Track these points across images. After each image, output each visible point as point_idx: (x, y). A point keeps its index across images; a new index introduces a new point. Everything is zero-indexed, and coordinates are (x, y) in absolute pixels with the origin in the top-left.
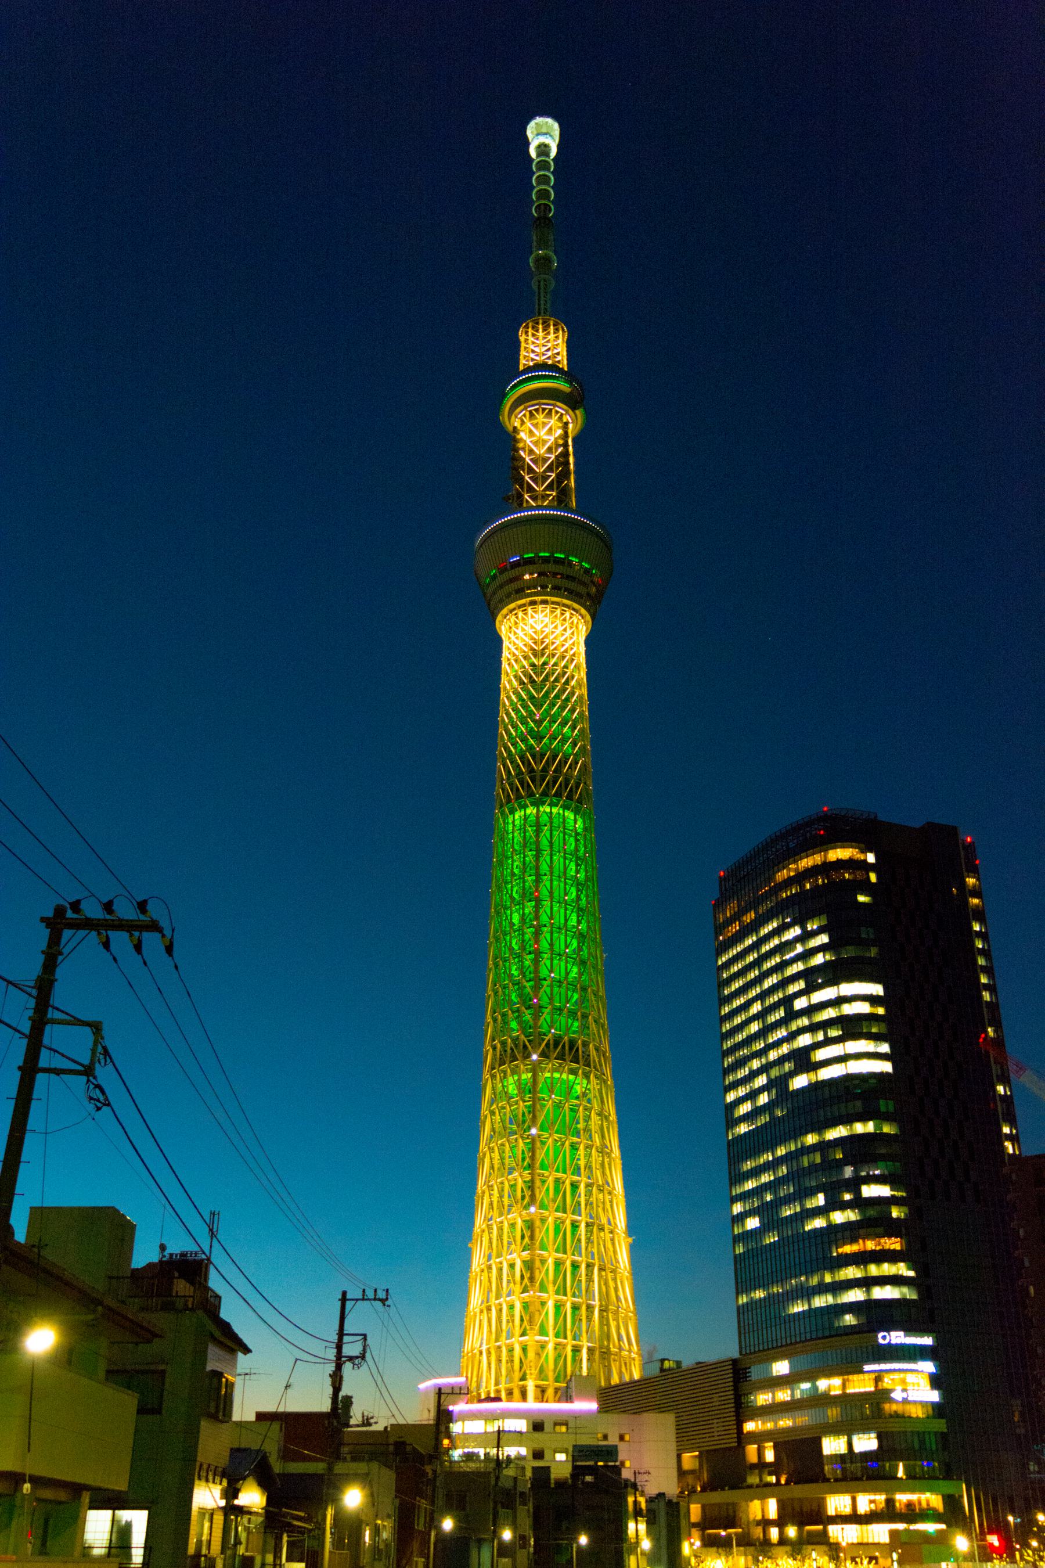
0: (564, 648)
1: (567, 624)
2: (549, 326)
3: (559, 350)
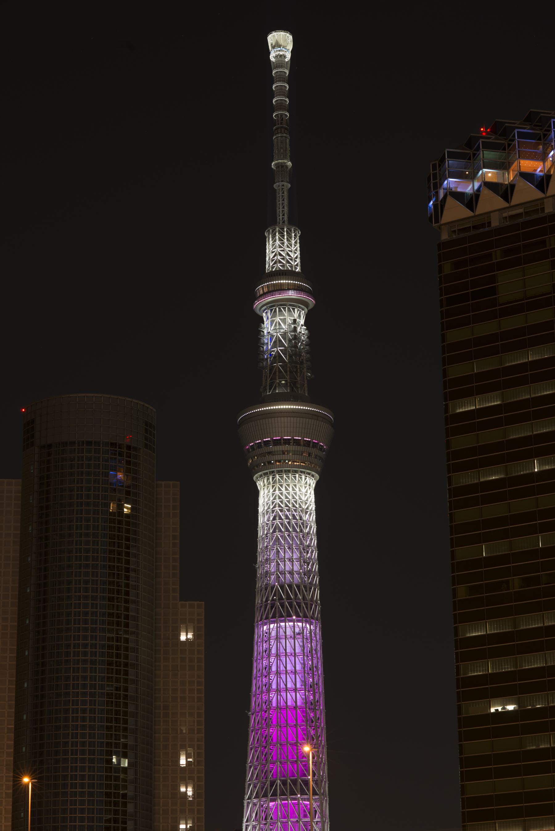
2: (275, 234)
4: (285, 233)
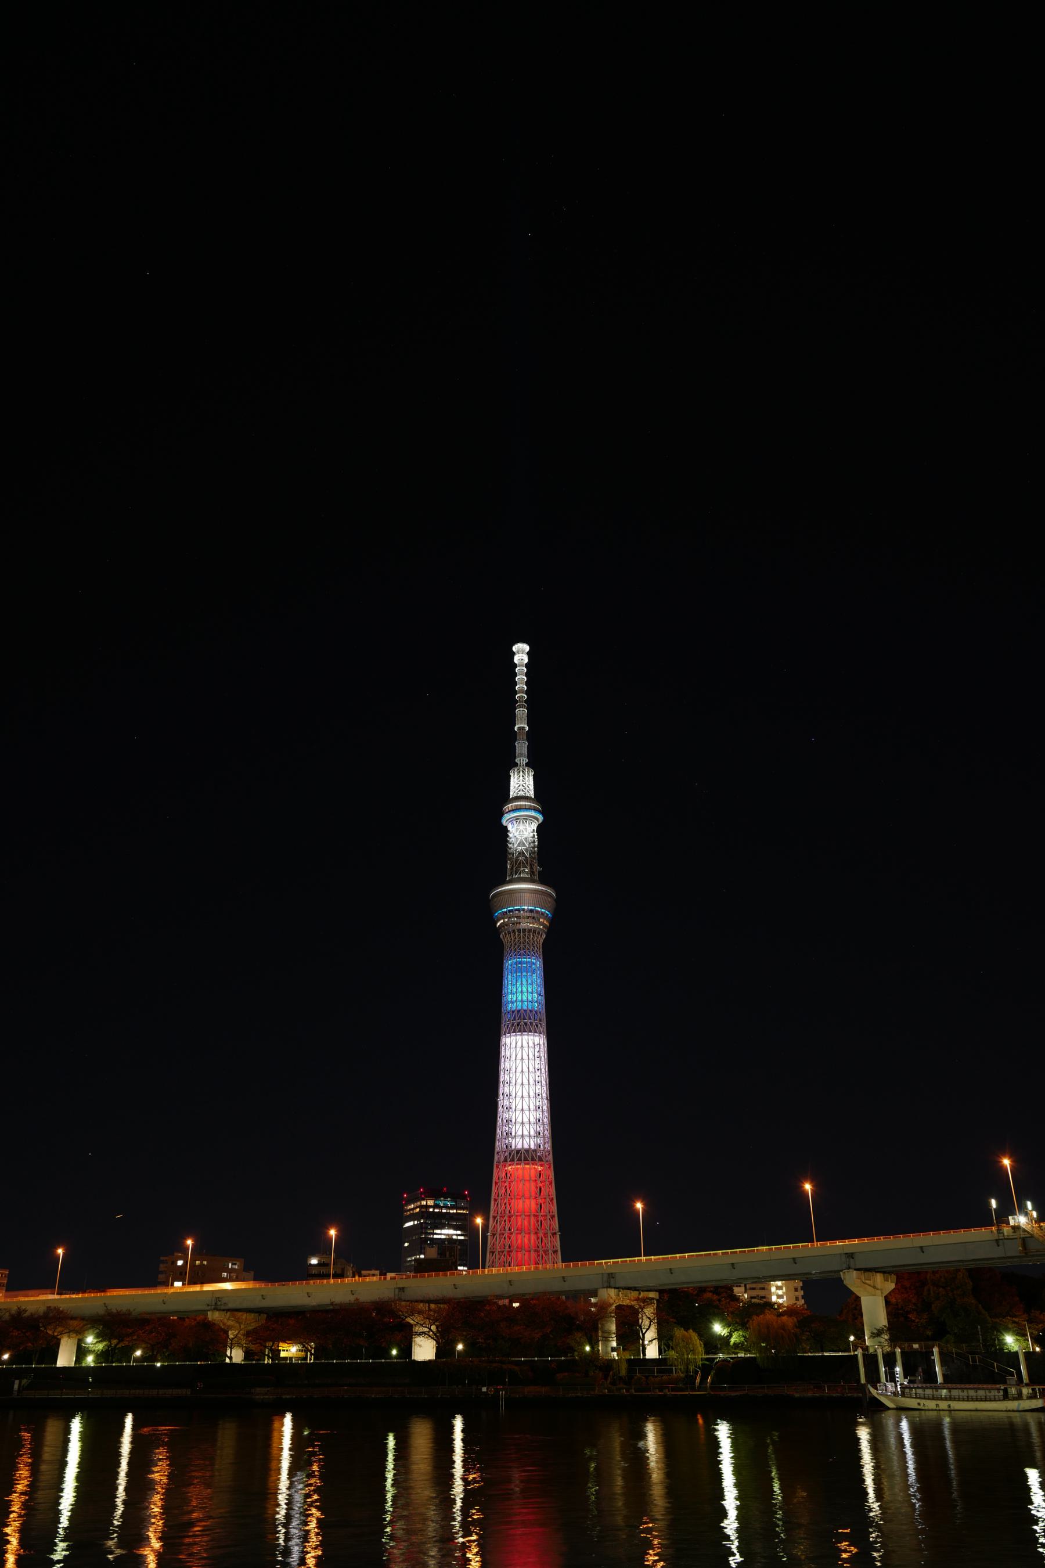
2: (519, 772)
4: (526, 772)
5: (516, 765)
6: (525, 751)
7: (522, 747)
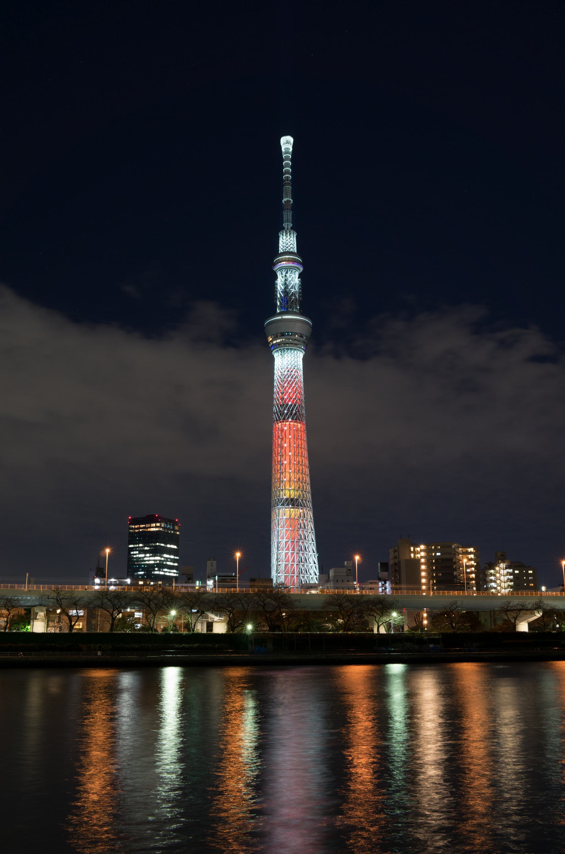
0: (291, 365)
1: (292, 356)
3: (292, 242)
5: (283, 228)
6: (290, 218)
7: (288, 215)
